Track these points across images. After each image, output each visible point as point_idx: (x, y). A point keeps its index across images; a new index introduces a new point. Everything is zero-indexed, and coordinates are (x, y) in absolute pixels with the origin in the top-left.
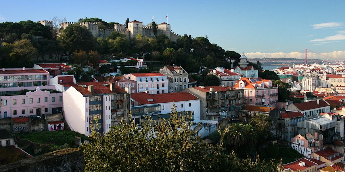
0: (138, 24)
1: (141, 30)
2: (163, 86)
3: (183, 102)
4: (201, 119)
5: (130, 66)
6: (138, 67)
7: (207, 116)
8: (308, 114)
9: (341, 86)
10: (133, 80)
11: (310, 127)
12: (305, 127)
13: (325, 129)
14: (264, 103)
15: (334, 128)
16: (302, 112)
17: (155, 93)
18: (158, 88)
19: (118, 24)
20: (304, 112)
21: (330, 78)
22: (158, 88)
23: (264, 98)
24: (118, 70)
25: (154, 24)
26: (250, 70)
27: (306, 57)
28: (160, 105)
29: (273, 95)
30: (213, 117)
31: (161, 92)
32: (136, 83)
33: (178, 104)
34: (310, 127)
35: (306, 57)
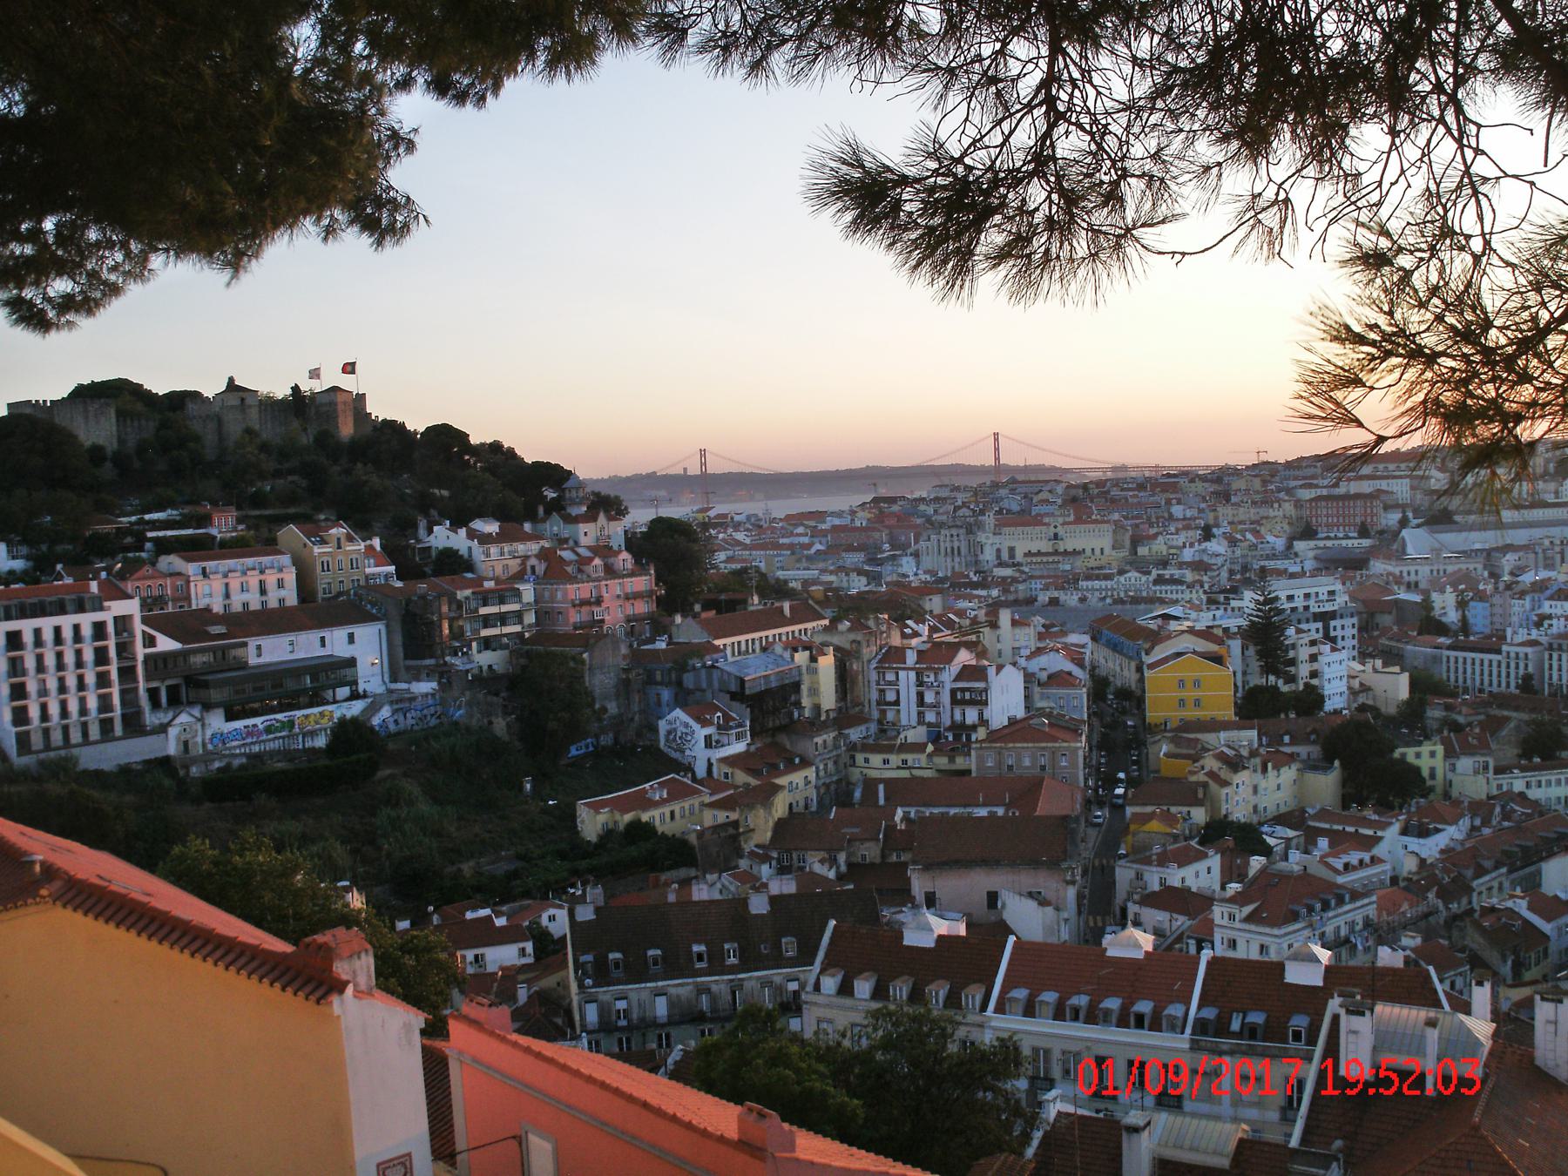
0: (244, 395)
1: (254, 414)
2: (280, 584)
3: (326, 633)
4: (394, 680)
5: (190, 532)
6: (214, 531)
7: (408, 668)
8: (743, 647)
9: (1039, 553)
10: (179, 574)
11: (716, 685)
12: (704, 685)
13: (758, 689)
14: (602, 621)
15: (796, 686)
16: (717, 642)
17: (255, 605)
18: (263, 592)
19: (195, 396)
20: (728, 641)
21: (1006, 530)
22: (263, 592)
23: (604, 605)
24: (148, 545)
25: (296, 389)
26: (595, 519)
27: (997, 459)
28: (245, 645)
29: (636, 596)
30: (424, 676)
31: (273, 604)
32: (188, 582)
33: (313, 637)
34: (716, 685)
35: (997, 459)
